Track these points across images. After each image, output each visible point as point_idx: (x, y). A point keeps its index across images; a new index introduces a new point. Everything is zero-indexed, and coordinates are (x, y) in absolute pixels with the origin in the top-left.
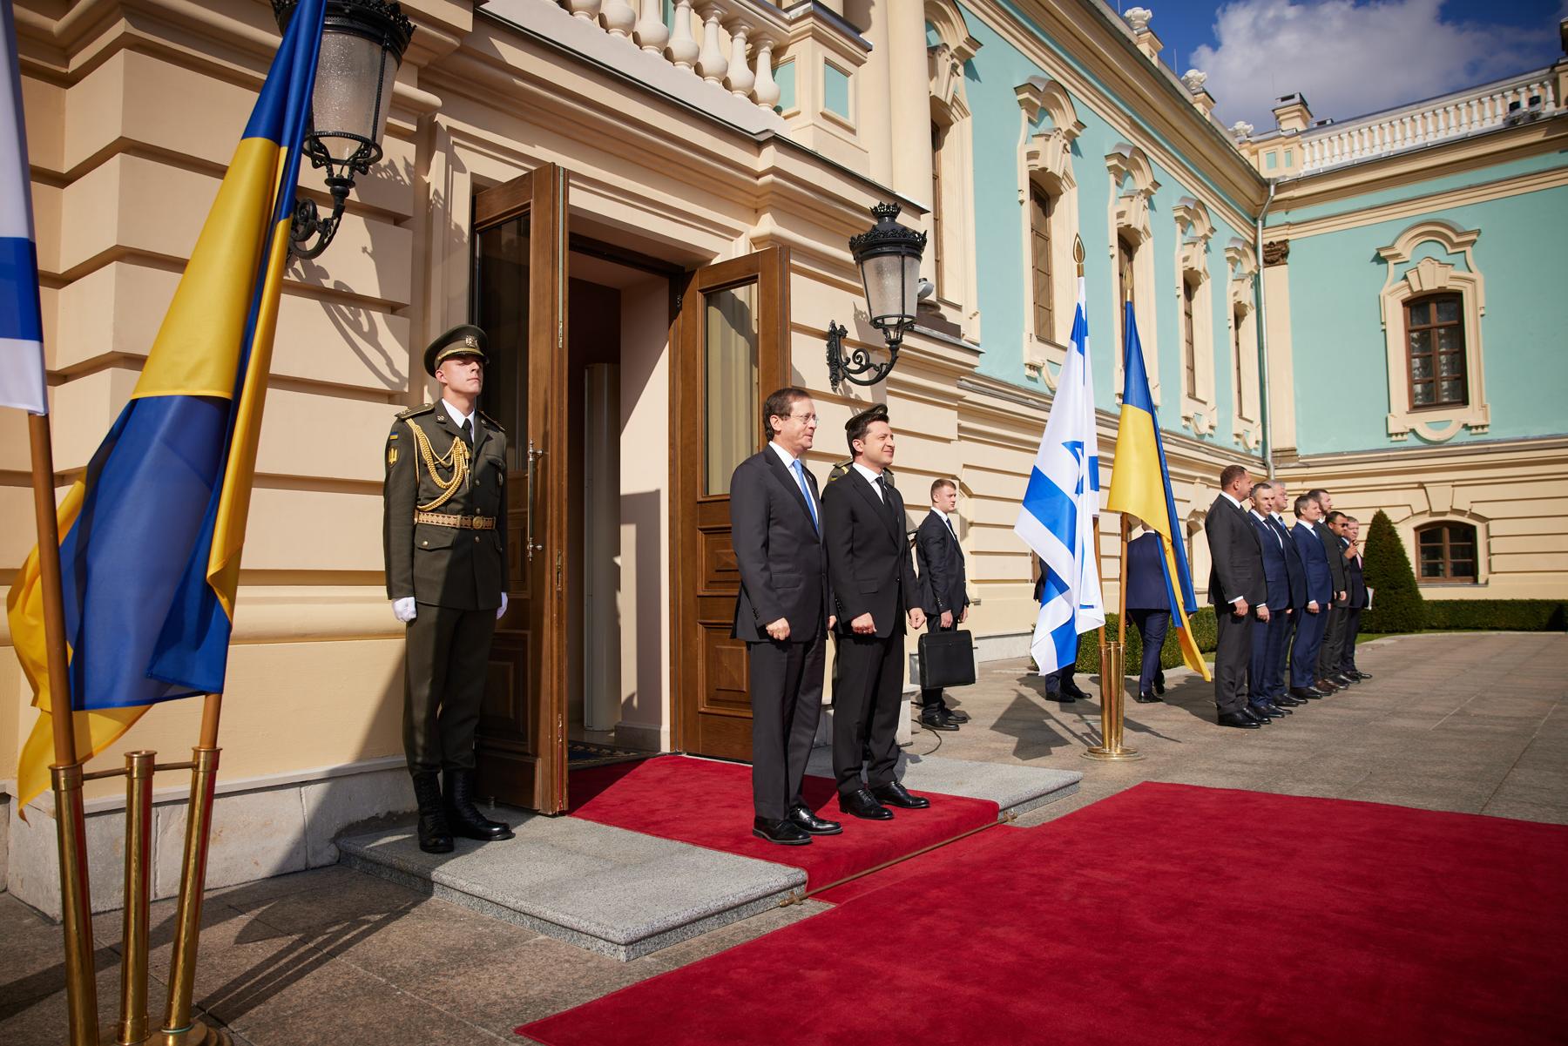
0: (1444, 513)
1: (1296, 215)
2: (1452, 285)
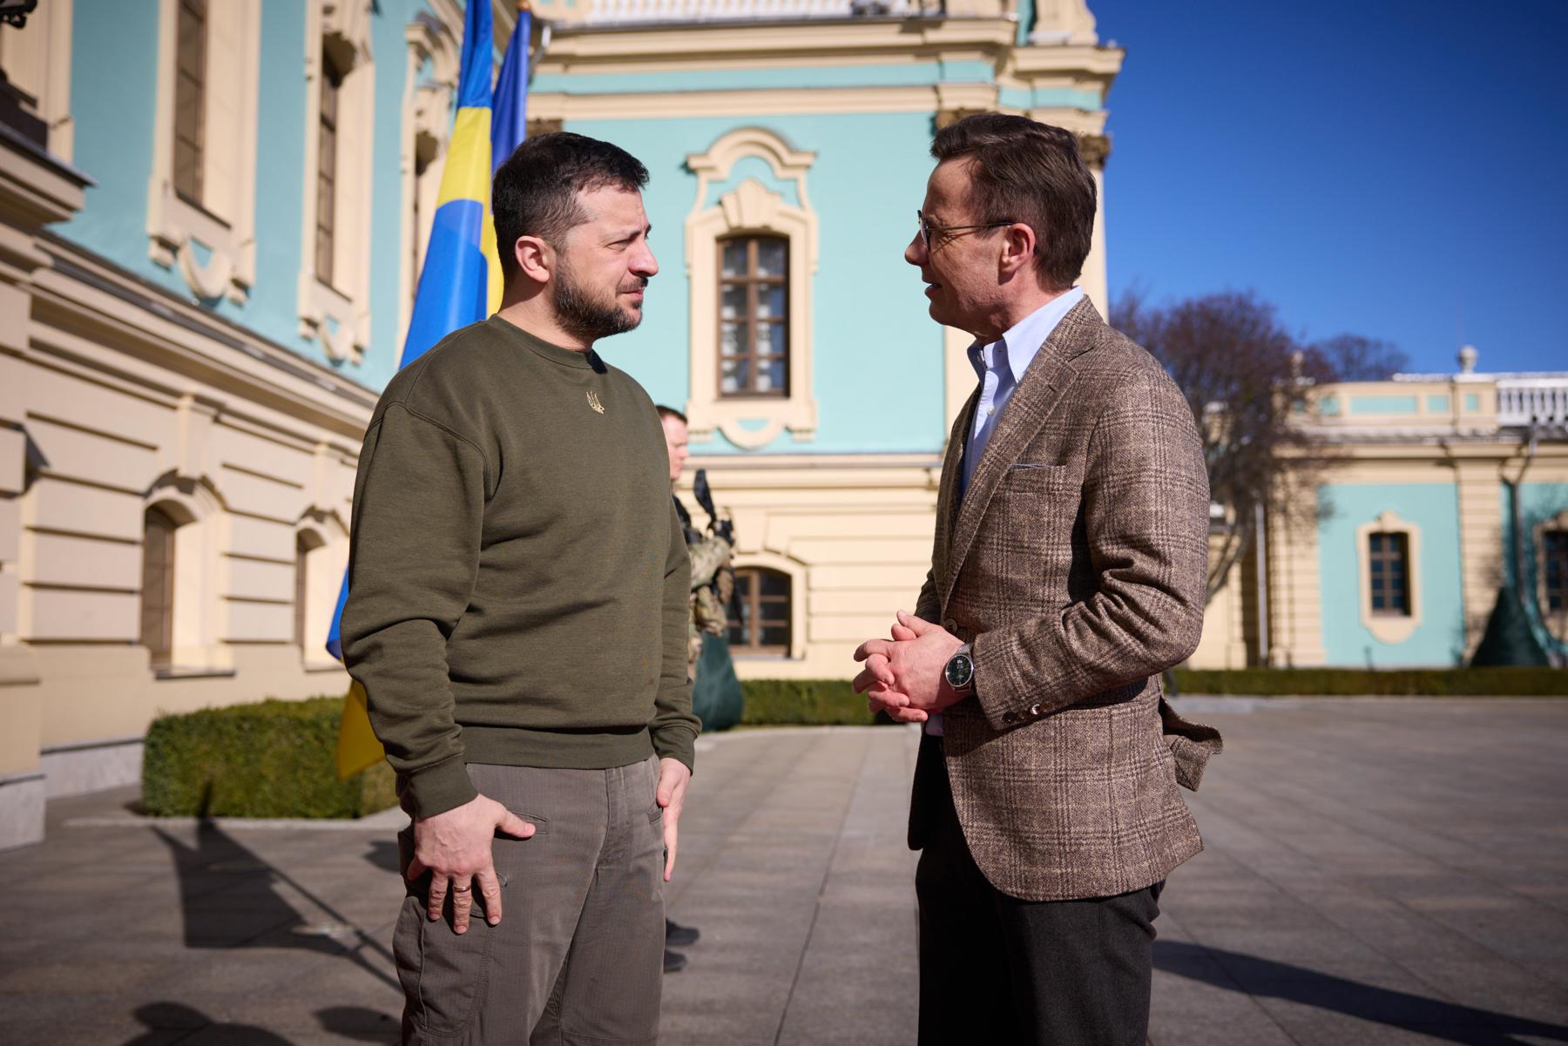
0: (753, 553)
1: (580, 78)
2: (779, 225)
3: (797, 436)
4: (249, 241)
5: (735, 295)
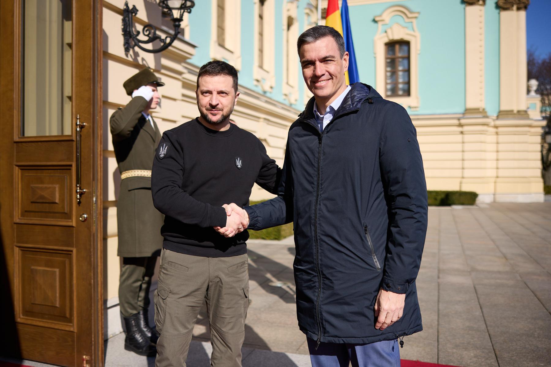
2: (406, 38)
3: (412, 109)
4: (239, 57)
5: (392, 63)
